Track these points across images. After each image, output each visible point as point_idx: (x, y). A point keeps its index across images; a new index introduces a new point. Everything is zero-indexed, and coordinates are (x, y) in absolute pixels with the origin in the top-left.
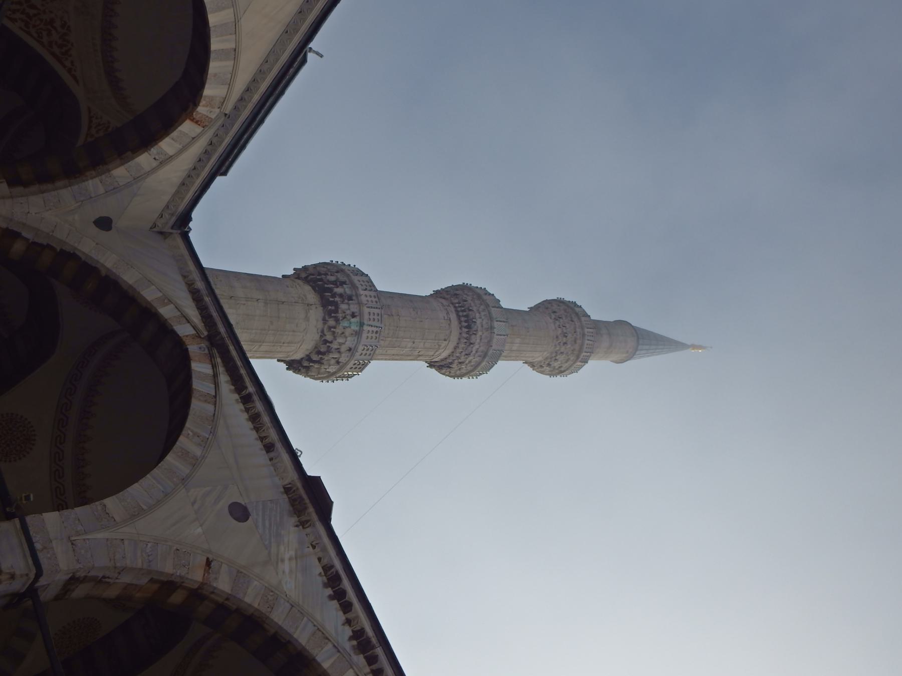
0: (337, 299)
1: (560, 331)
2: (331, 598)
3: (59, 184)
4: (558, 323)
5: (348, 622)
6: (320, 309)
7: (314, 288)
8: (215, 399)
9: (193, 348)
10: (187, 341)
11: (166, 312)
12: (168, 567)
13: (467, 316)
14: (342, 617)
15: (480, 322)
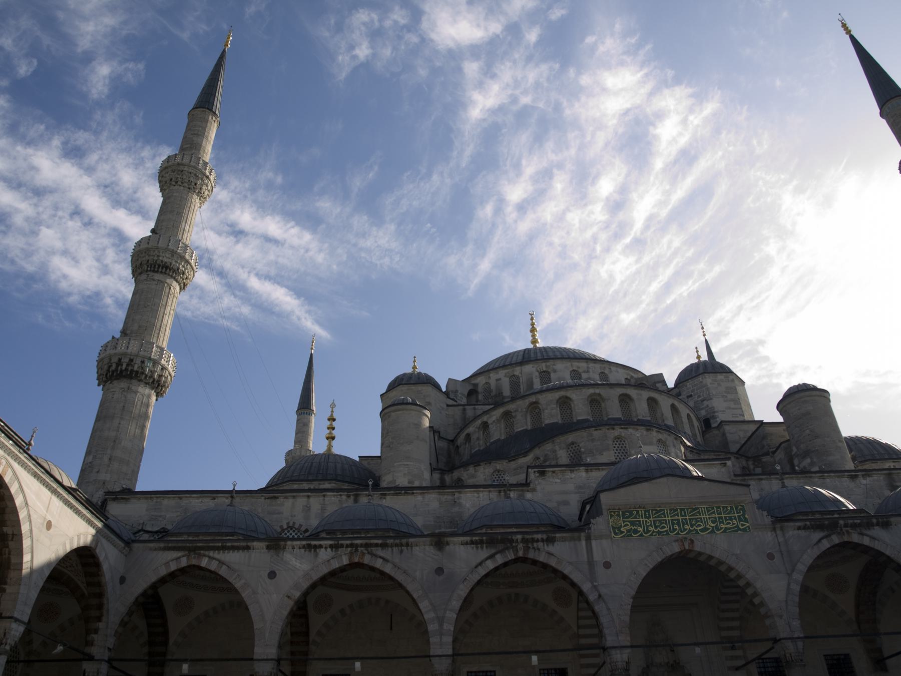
0: (130, 368)
1: (186, 185)
2: (315, 551)
3: (105, 602)
4: (179, 183)
5: (326, 548)
6: (133, 381)
7: (117, 379)
8: (221, 563)
9: (194, 562)
10: (190, 563)
11: (173, 567)
12: (285, 613)
13: (159, 266)
14: (323, 550)
15: (166, 258)
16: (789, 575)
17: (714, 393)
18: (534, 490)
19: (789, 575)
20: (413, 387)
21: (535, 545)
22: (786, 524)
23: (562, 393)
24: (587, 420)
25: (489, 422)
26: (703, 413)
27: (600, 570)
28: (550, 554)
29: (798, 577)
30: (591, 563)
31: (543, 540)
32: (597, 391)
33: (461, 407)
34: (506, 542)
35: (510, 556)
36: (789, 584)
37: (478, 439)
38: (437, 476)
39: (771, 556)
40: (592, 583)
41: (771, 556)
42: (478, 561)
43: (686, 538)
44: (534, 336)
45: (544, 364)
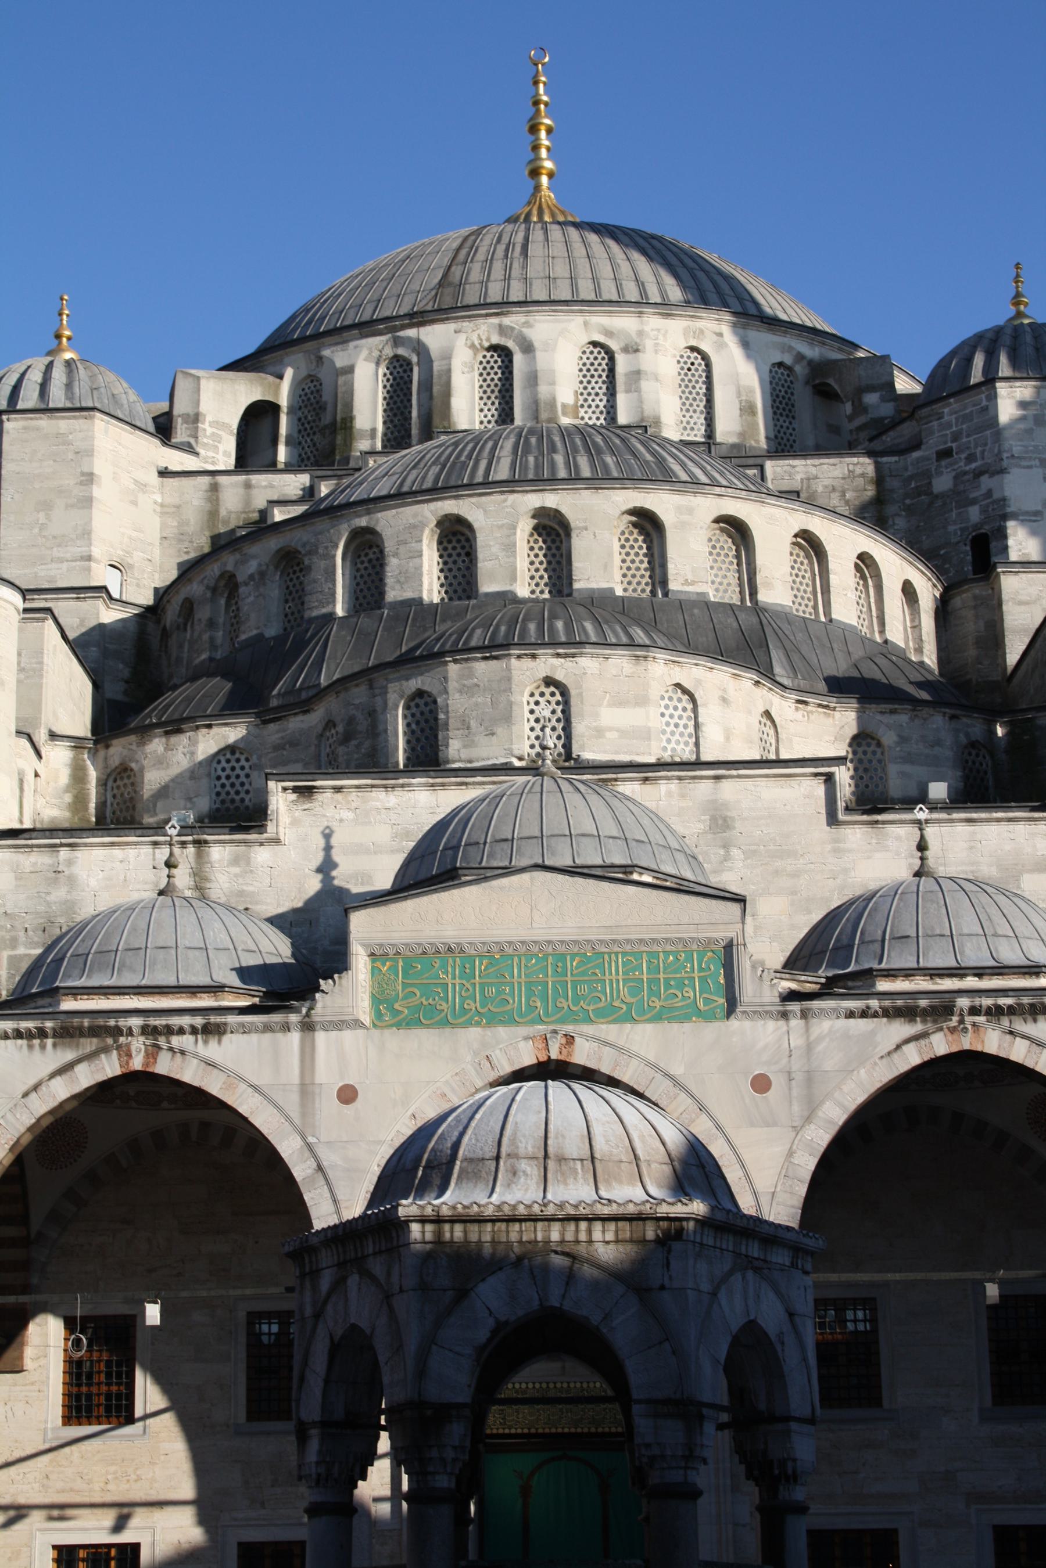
16: (797, 1130)
17: (1017, 450)
18: (277, 841)
19: (797, 1130)
20: (43, 422)
21: (176, 1041)
22: (816, 1004)
23: (449, 506)
24: (507, 598)
25: (241, 578)
26: (974, 514)
27: (328, 1105)
28: (211, 1064)
29: (820, 1137)
30: (307, 1090)
31: (194, 1031)
32: (551, 500)
33: (206, 480)
34: (103, 1030)
35: (109, 1067)
36: (790, 1153)
37: (211, 624)
38: (59, 756)
39: (761, 1084)
40: (304, 1138)
41: (761, 1084)
42: (32, 1082)
43: (555, 1032)
44: (536, 148)
45: (495, 321)
